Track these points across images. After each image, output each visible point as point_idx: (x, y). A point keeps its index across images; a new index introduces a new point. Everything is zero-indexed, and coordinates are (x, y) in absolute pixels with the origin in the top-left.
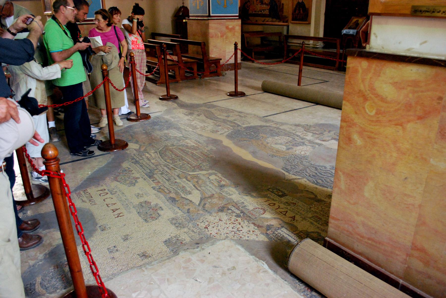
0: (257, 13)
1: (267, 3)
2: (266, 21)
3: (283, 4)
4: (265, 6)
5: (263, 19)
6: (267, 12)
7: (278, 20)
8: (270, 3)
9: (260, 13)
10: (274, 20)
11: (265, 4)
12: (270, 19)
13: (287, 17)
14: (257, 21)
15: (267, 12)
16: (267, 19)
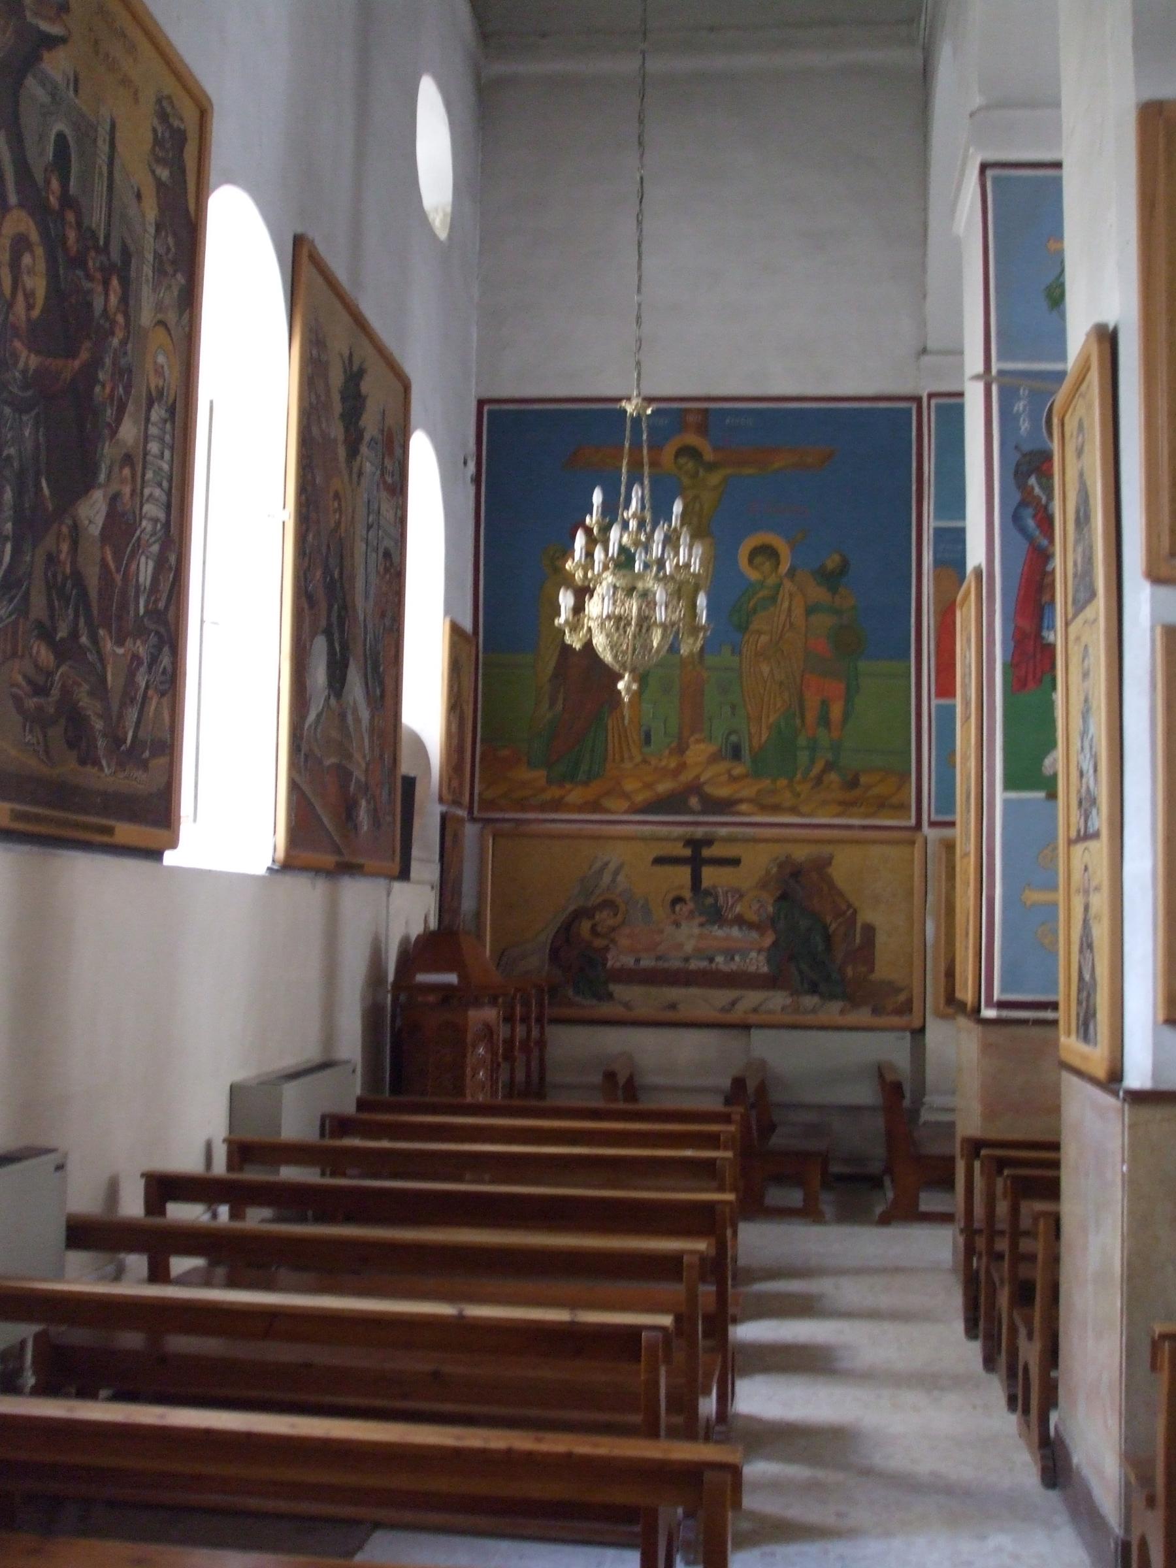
0: (676, 964)
1: (751, 916)
2: (741, 1007)
3: (870, 930)
4: (735, 932)
5: (722, 997)
6: (757, 963)
7: (835, 1006)
8: (773, 921)
9: (694, 965)
10: (810, 1001)
11: (740, 921)
12: (778, 1000)
13: (899, 990)
14: (673, 1006)
15: (757, 963)
16: (753, 997)
